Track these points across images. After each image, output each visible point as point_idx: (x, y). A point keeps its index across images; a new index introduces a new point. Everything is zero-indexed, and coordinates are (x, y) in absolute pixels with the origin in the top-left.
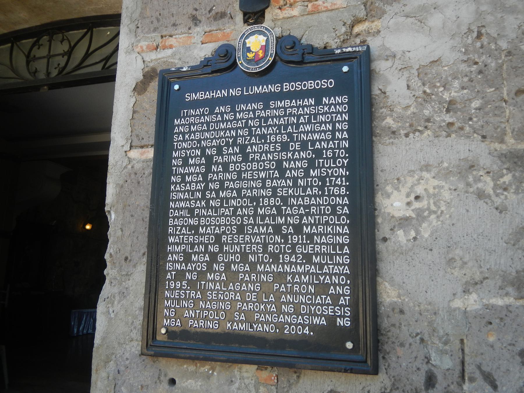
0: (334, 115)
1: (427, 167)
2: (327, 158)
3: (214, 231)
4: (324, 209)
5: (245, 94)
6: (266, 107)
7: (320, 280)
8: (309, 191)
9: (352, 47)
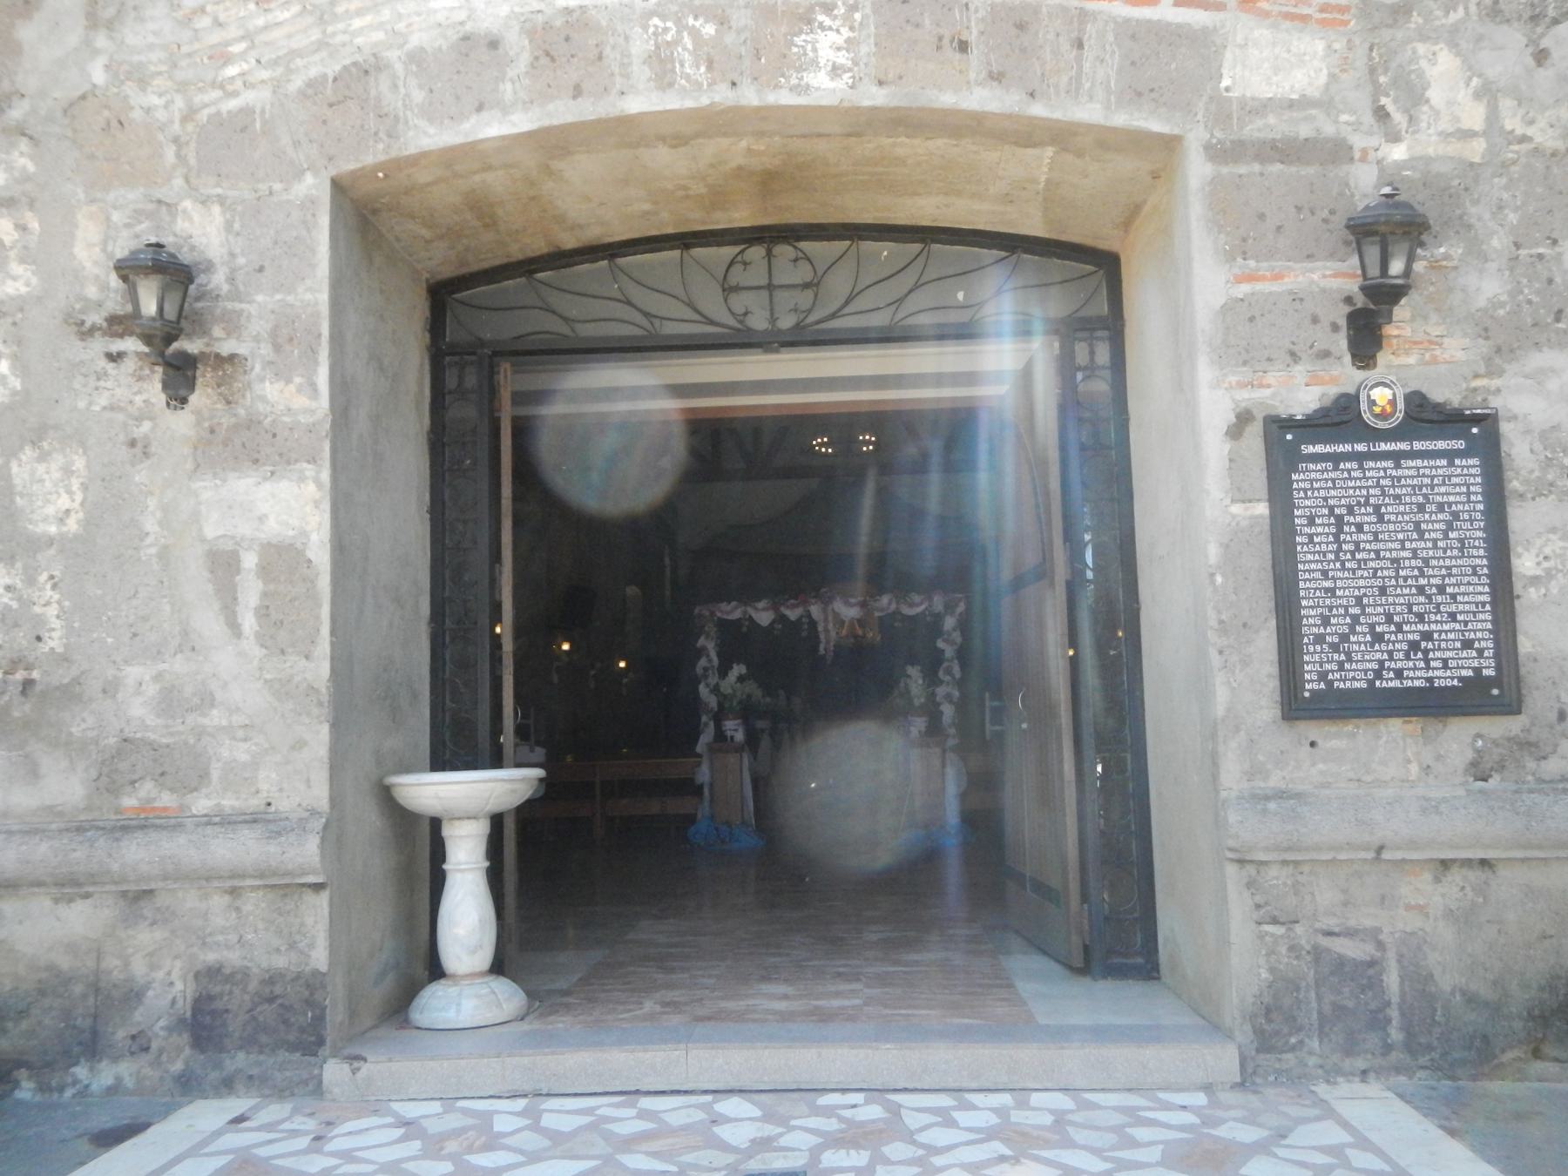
1: (1553, 530)
6: (1398, 466)
8: (1449, 553)
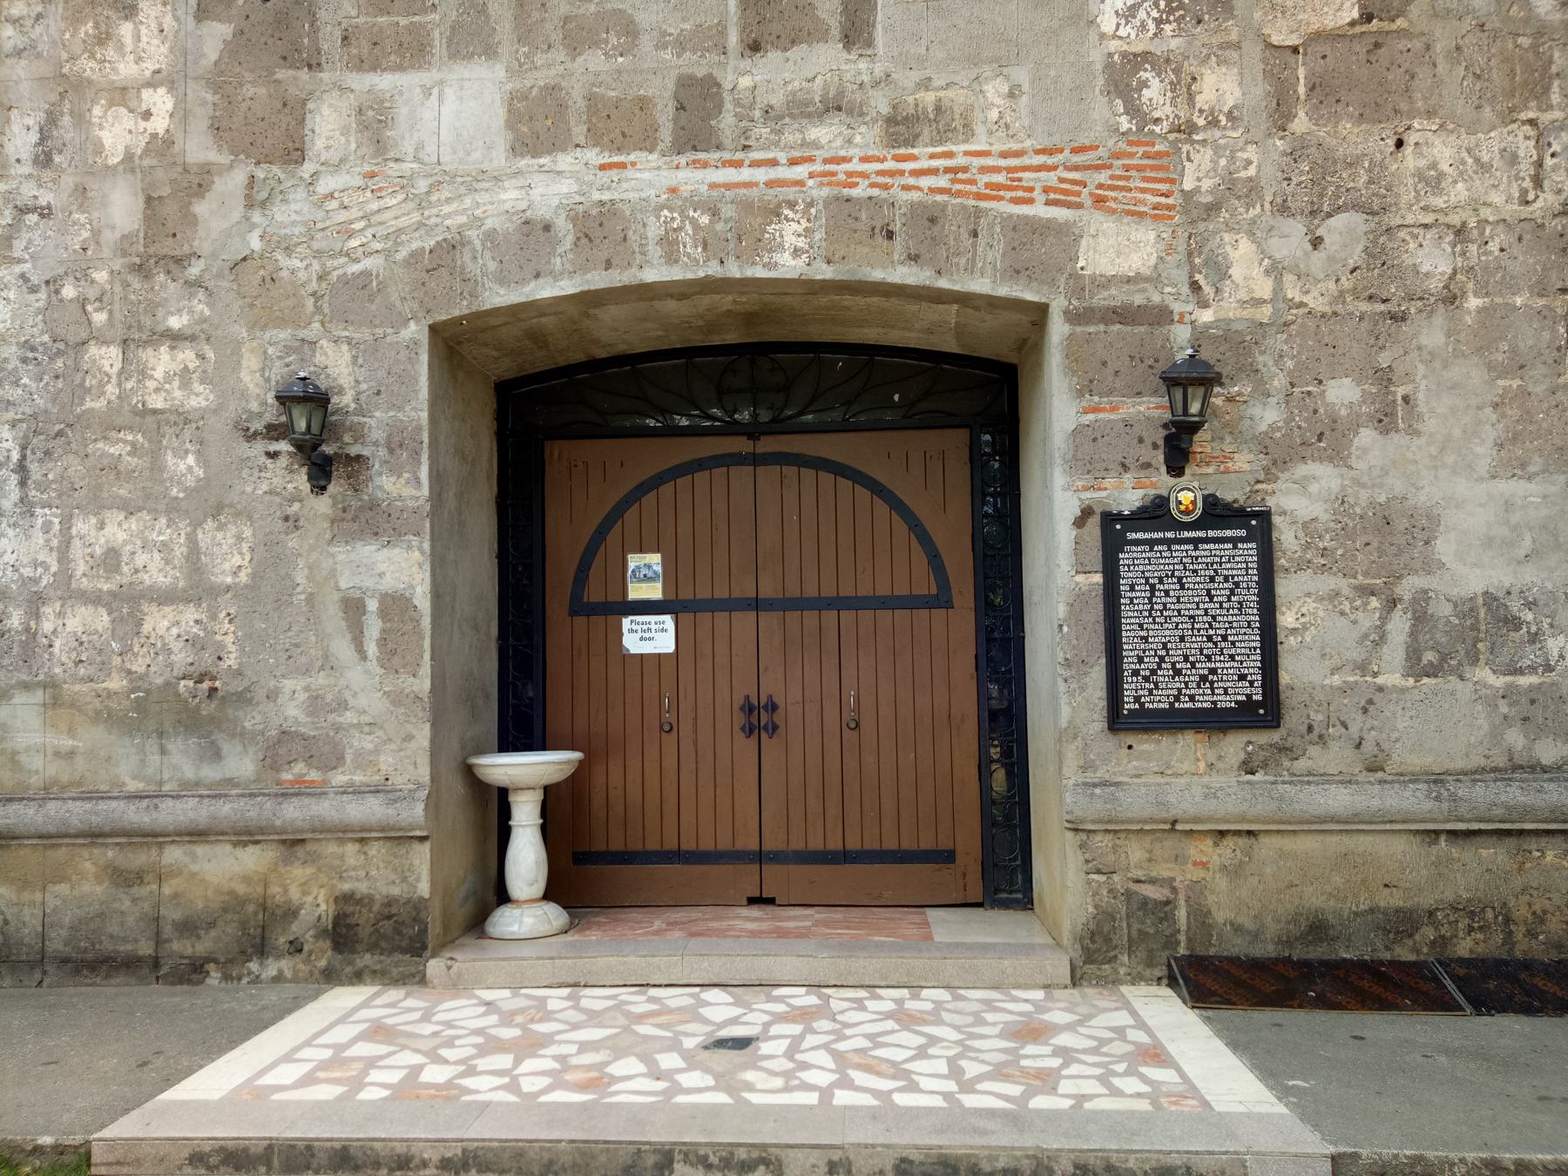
1: (1309, 595)
6: (1196, 549)
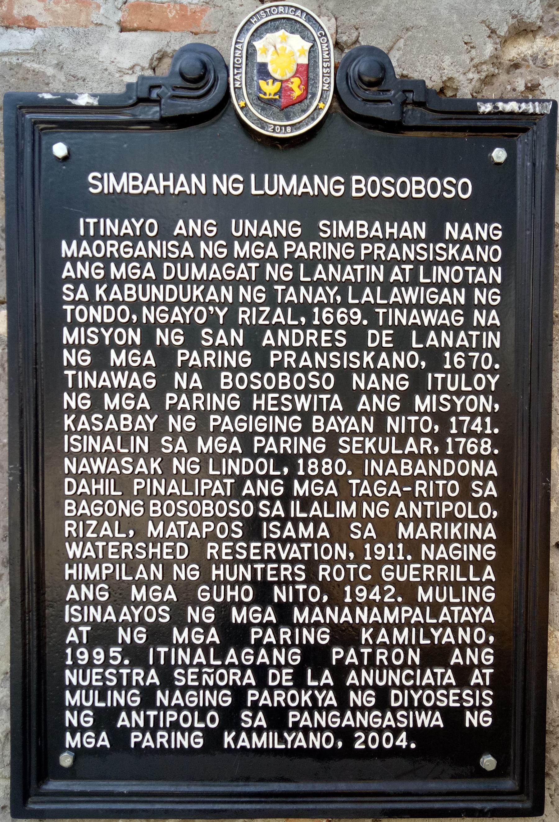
0: (470, 269)
2: (453, 371)
3: (186, 533)
4: (445, 486)
5: (254, 192)
6: (310, 234)
7: (431, 637)
8: (411, 445)
9: (519, 101)
